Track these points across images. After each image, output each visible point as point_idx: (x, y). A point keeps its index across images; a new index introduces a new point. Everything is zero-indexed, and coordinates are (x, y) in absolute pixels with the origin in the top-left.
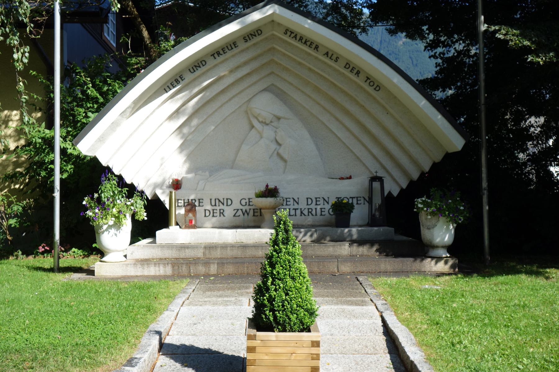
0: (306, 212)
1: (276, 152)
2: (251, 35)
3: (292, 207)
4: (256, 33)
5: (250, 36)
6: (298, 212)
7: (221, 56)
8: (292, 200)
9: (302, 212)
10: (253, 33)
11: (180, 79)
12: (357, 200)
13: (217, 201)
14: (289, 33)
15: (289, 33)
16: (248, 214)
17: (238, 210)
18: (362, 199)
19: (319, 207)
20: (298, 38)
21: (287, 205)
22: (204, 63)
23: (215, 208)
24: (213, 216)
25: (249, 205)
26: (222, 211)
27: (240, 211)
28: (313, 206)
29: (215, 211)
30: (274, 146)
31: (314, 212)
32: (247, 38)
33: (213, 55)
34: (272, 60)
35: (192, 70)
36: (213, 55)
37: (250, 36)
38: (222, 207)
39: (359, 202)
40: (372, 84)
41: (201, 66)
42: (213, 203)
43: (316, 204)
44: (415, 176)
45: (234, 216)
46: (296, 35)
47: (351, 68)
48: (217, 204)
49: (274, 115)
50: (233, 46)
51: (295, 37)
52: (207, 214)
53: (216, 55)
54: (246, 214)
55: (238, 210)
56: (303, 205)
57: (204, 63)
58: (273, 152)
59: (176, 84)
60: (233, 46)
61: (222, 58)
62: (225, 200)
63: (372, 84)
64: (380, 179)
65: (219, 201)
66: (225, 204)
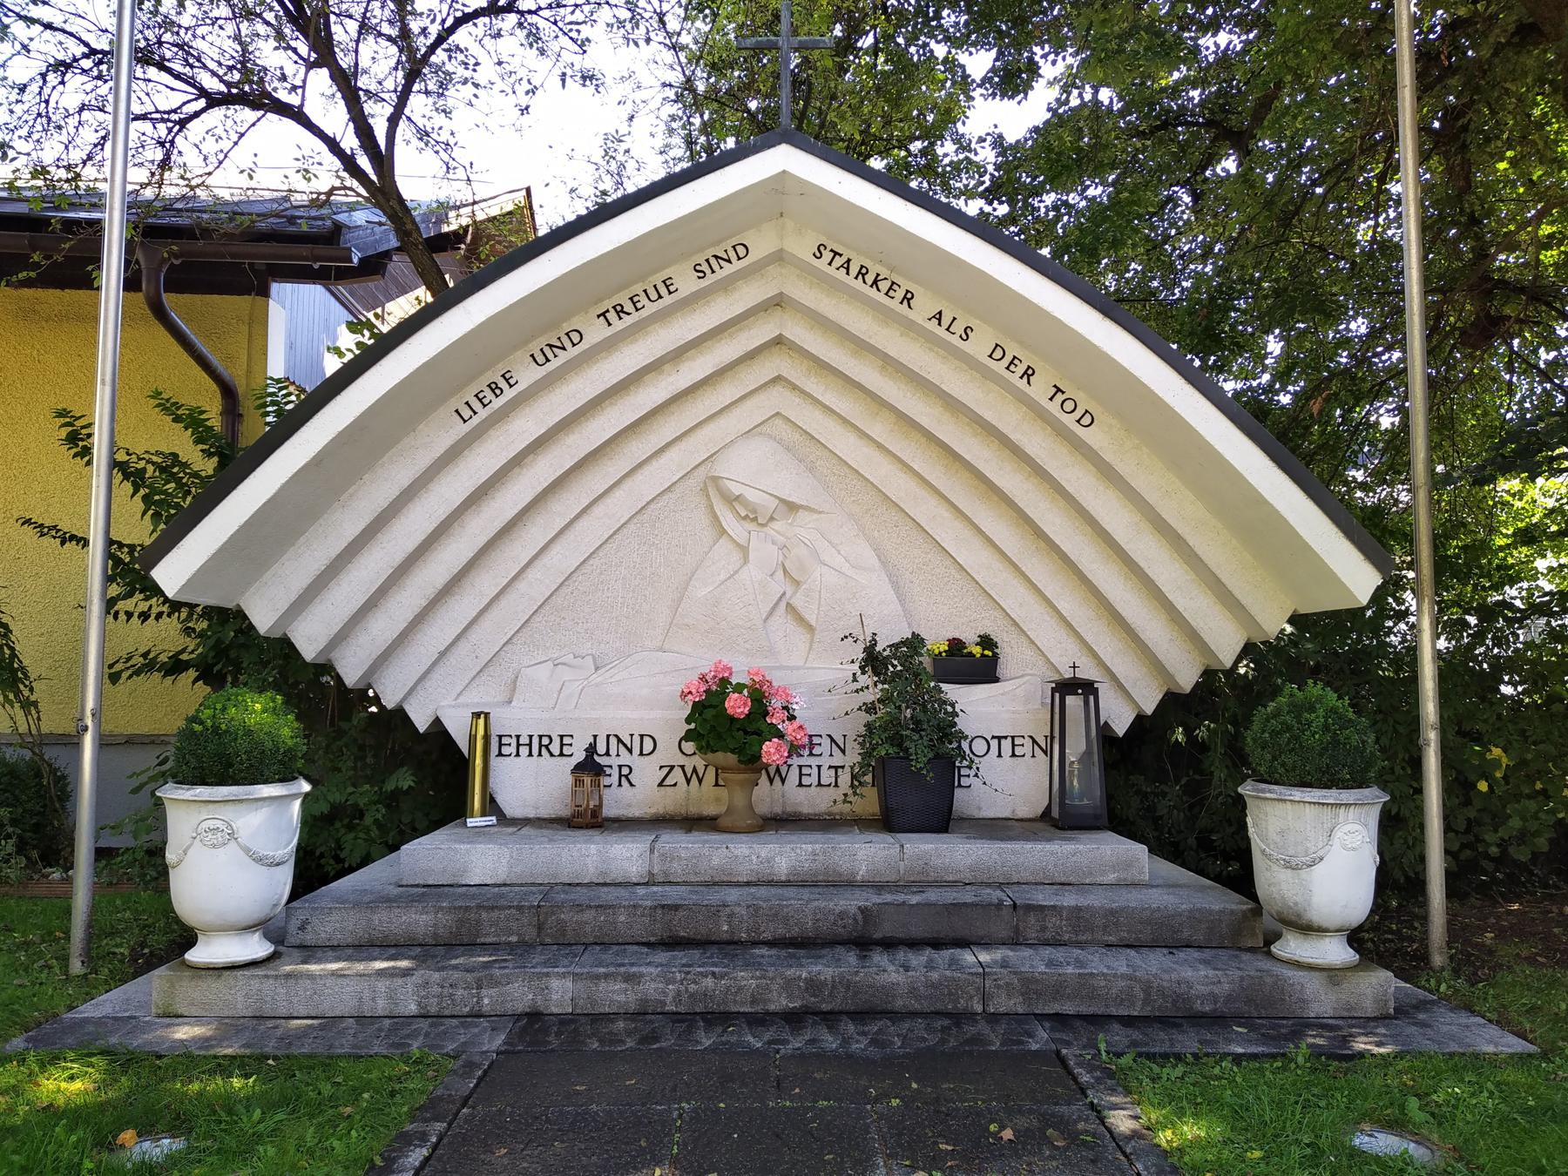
1: (783, 605)
3: (826, 762)
11: (503, 384)
12: (1014, 745)
13: (613, 741)
15: (827, 255)
16: (700, 781)
17: (672, 767)
18: (1028, 742)
26: (625, 771)
27: (678, 771)
30: (778, 586)
32: (705, 267)
34: (779, 341)
37: (713, 261)
38: (625, 758)
40: (1069, 406)
41: (568, 344)
44: (1187, 679)
45: (660, 785)
46: (849, 261)
47: (1008, 359)
48: (613, 751)
49: (782, 500)
50: (663, 291)
51: (847, 266)
55: (672, 767)
58: (777, 604)
60: (663, 291)
62: (637, 739)
63: (1069, 406)
64: (1087, 688)
65: (620, 741)
66: (636, 750)
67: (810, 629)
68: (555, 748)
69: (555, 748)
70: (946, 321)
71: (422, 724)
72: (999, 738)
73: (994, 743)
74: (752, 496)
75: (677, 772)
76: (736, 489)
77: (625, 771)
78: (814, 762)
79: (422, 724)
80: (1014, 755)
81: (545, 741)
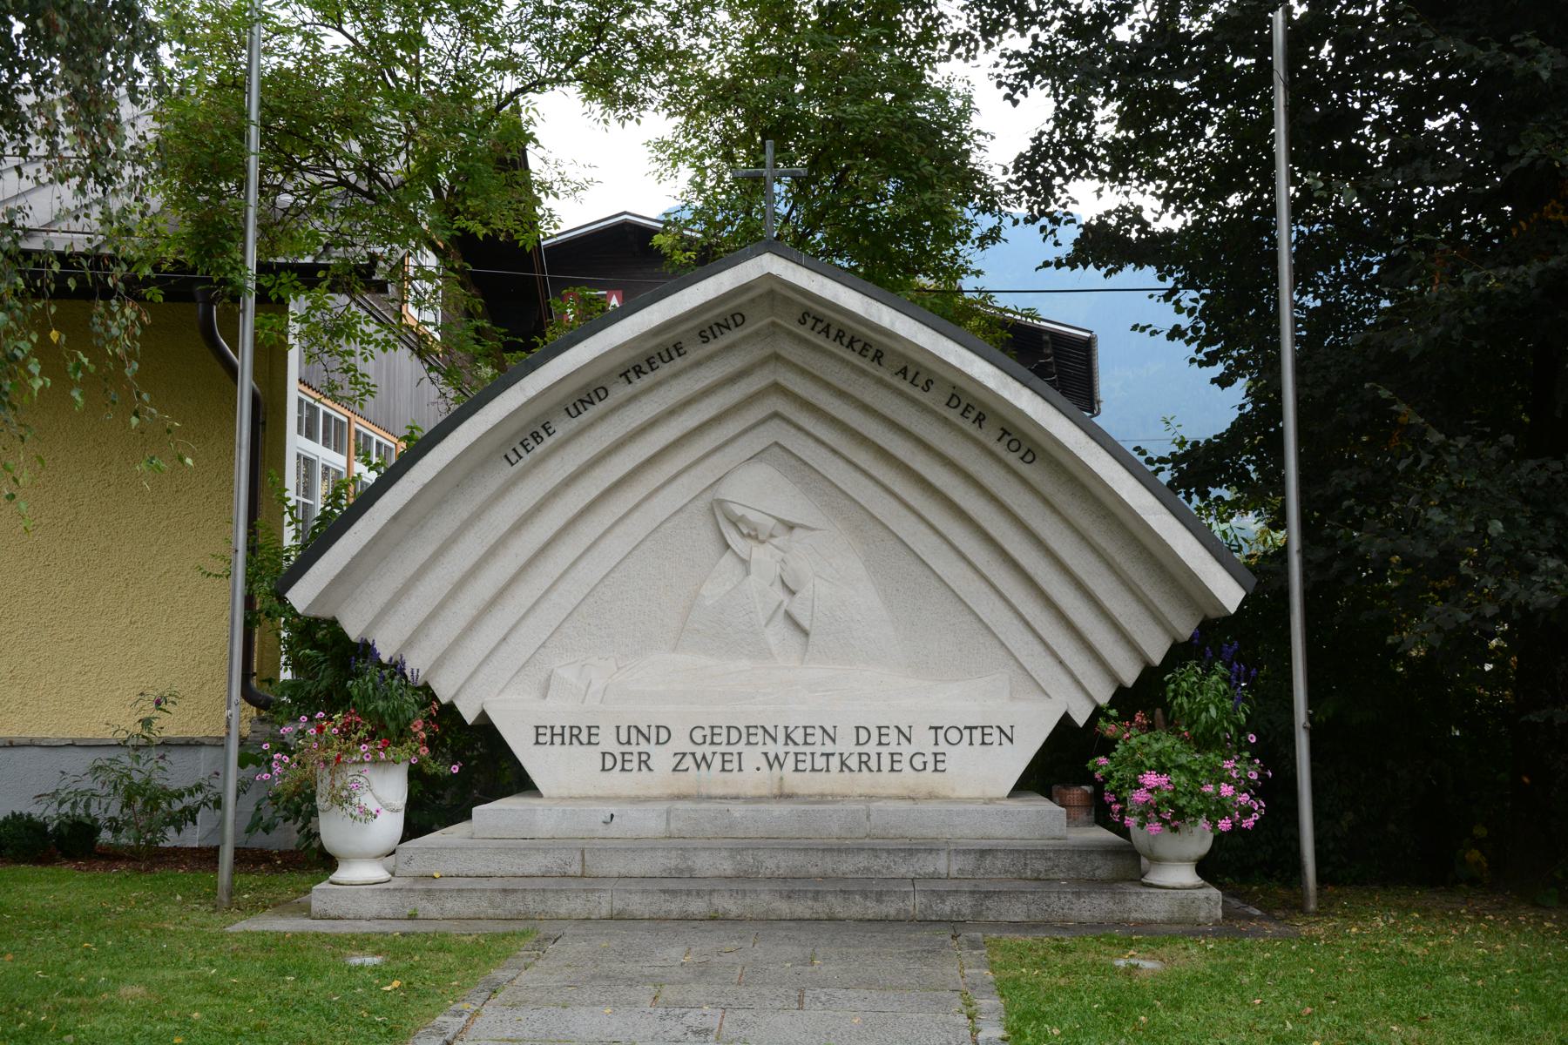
0: (853, 762)
1: (782, 611)
2: (718, 325)
3: (818, 749)
4: (731, 322)
5: (715, 329)
6: (835, 762)
7: (644, 377)
8: (819, 732)
9: (843, 763)
10: (722, 322)
13: (634, 732)
14: (810, 322)
15: (810, 322)
19: (885, 751)
20: (833, 332)
21: (806, 743)
22: (602, 394)
23: (627, 748)
24: (623, 769)
25: (712, 743)
26: (644, 757)
27: (689, 758)
28: (872, 748)
29: (627, 757)
30: (779, 594)
31: (873, 764)
32: (708, 333)
33: (625, 374)
35: (572, 410)
36: (625, 374)
37: (715, 329)
38: (644, 746)
39: (987, 740)
42: (624, 739)
43: (880, 743)
44: (1129, 674)
45: (674, 770)
48: (633, 740)
49: (779, 520)
50: (674, 354)
52: (609, 763)
53: (632, 375)
54: (703, 765)
55: (684, 754)
56: (846, 744)
57: (602, 394)
58: (775, 612)
59: (533, 443)
60: (674, 354)
61: (646, 380)
62: (653, 730)
65: (639, 731)
67: (806, 633)
68: (584, 737)
69: (584, 737)
70: (910, 375)
71: (470, 717)
72: (971, 728)
73: (966, 733)
74: (753, 516)
75: (689, 758)
76: (739, 511)
77: (644, 757)
78: (808, 749)
79: (470, 717)
80: (983, 743)
81: (575, 731)
